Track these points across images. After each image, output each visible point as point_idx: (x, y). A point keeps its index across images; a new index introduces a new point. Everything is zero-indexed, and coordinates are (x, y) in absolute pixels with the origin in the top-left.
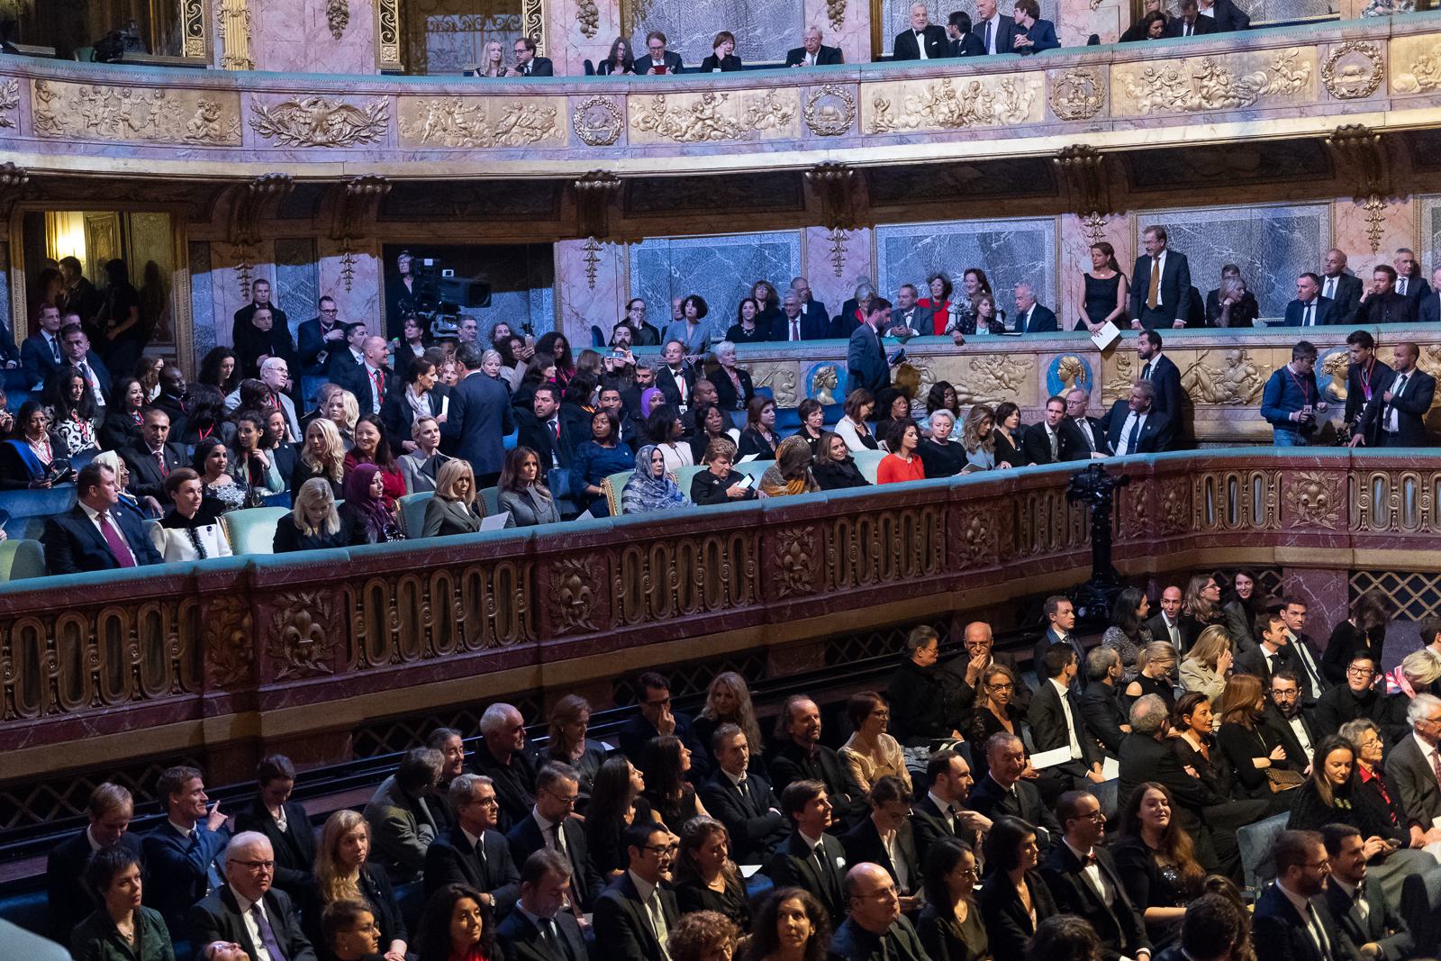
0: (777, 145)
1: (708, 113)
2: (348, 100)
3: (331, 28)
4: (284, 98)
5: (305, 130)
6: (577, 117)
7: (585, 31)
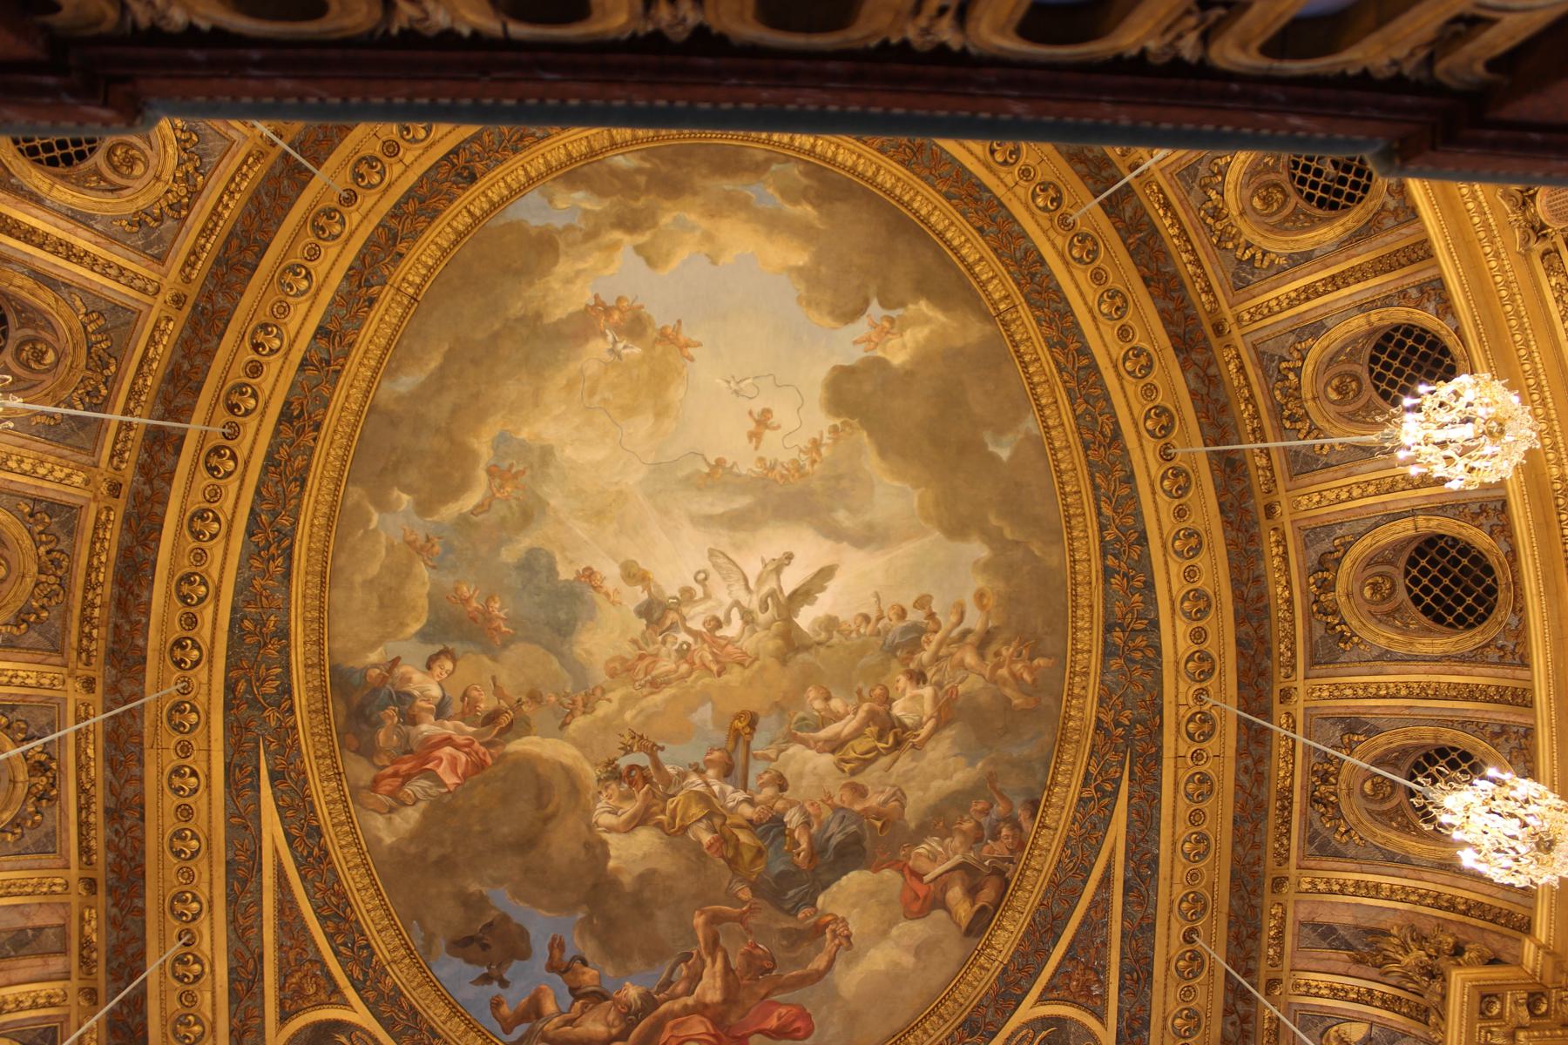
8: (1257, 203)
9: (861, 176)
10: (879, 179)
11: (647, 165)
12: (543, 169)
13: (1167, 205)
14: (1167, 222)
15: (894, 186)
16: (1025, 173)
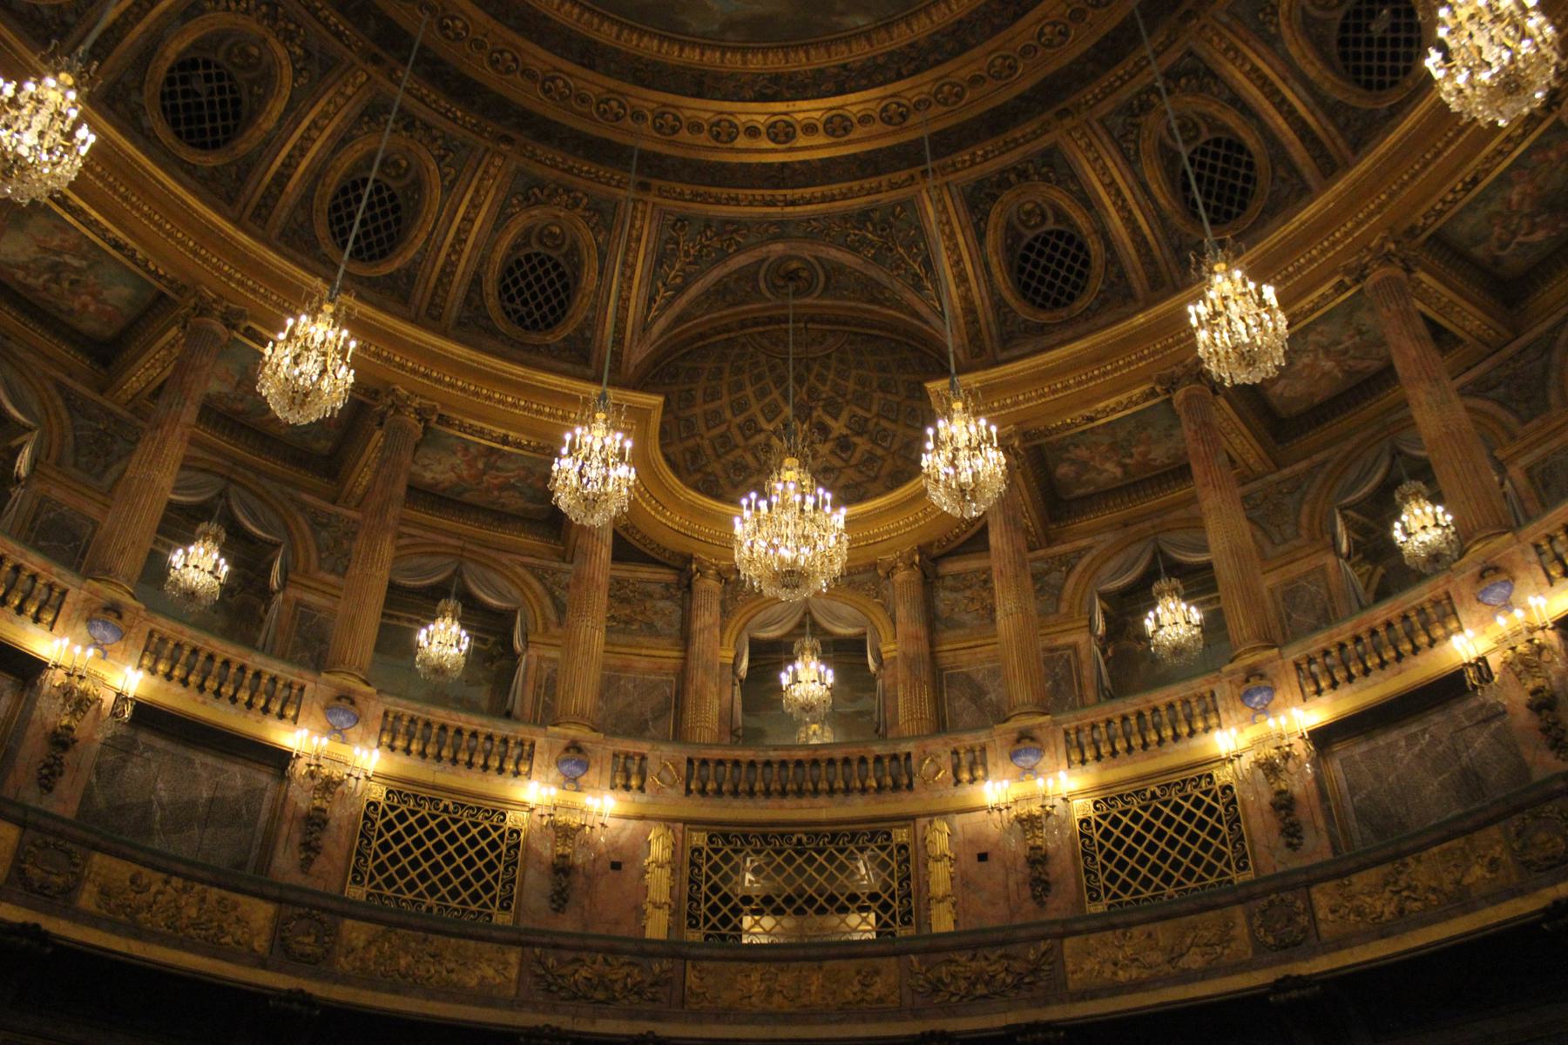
0: (1493, 899)
1: (1402, 884)
3: (1034, 897)
5: (963, 984)
6: (1256, 922)
7: (1289, 845)
8: (255, 52)
9: (632, 29)
10: (615, 29)
11: (835, 19)
12: (933, 10)
13: (339, 35)
14: (333, 20)
15: (601, 23)
16: (481, 46)
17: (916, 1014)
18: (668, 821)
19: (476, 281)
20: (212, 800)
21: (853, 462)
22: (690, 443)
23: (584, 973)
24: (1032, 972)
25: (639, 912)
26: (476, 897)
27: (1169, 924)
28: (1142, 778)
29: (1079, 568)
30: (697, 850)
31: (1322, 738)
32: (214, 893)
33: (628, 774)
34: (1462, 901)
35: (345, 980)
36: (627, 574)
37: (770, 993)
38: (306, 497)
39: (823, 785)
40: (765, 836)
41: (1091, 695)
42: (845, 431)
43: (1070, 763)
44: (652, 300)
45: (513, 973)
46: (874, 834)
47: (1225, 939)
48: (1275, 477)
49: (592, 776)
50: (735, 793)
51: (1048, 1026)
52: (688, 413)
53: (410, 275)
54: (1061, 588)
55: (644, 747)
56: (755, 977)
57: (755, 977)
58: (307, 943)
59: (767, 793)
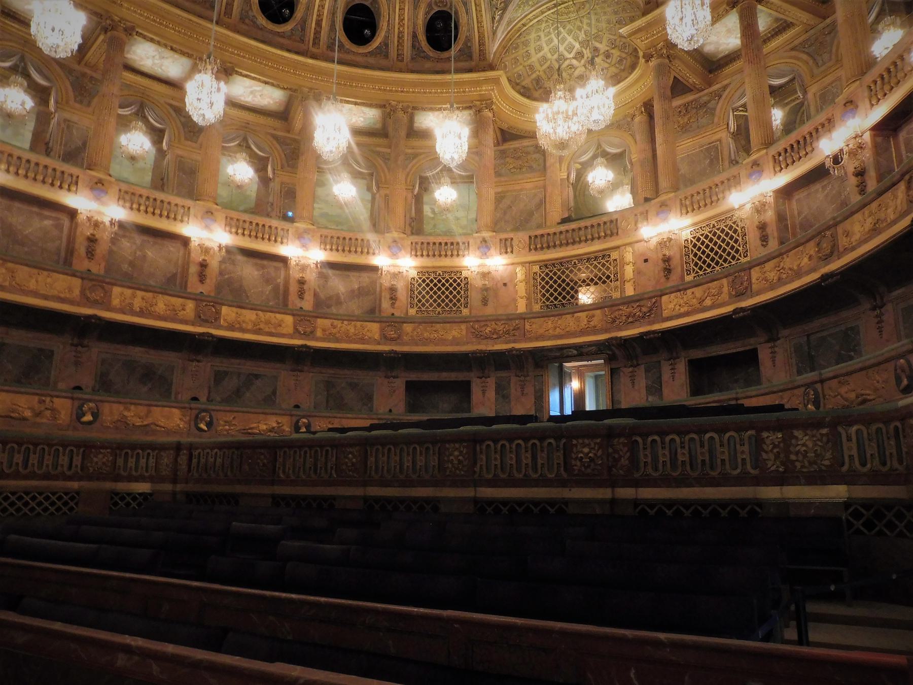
2: (642, 303)
4: (617, 308)
5: (624, 318)
17: (607, 331)
18: (523, 264)
19: (415, 36)
20: (359, 288)
21: (613, 63)
22: (534, 76)
23: (489, 329)
24: (649, 311)
25: (515, 300)
26: (455, 305)
27: (700, 287)
28: (710, 219)
29: (724, 97)
30: (536, 273)
31: (786, 193)
32: (359, 324)
33: (506, 247)
34: (798, 274)
35: (406, 344)
36: (517, 146)
37: (555, 328)
38: (378, 149)
39: (583, 238)
40: (561, 263)
41: (727, 163)
42: (607, 48)
43: (682, 214)
44: (493, 18)
45: (464, 333)
46: (604, 256)
47: (720, 293)
48: (822, 25)
49: (493, 251)
50: (548, 247)
51: (654, 332)
52: (529, 62)
53: (385, 44)
54: (714, 109)
55: (511, 235)
56: (550, 322)
57: (550, 322)
58: (392, 334)
59: (561, 245)
